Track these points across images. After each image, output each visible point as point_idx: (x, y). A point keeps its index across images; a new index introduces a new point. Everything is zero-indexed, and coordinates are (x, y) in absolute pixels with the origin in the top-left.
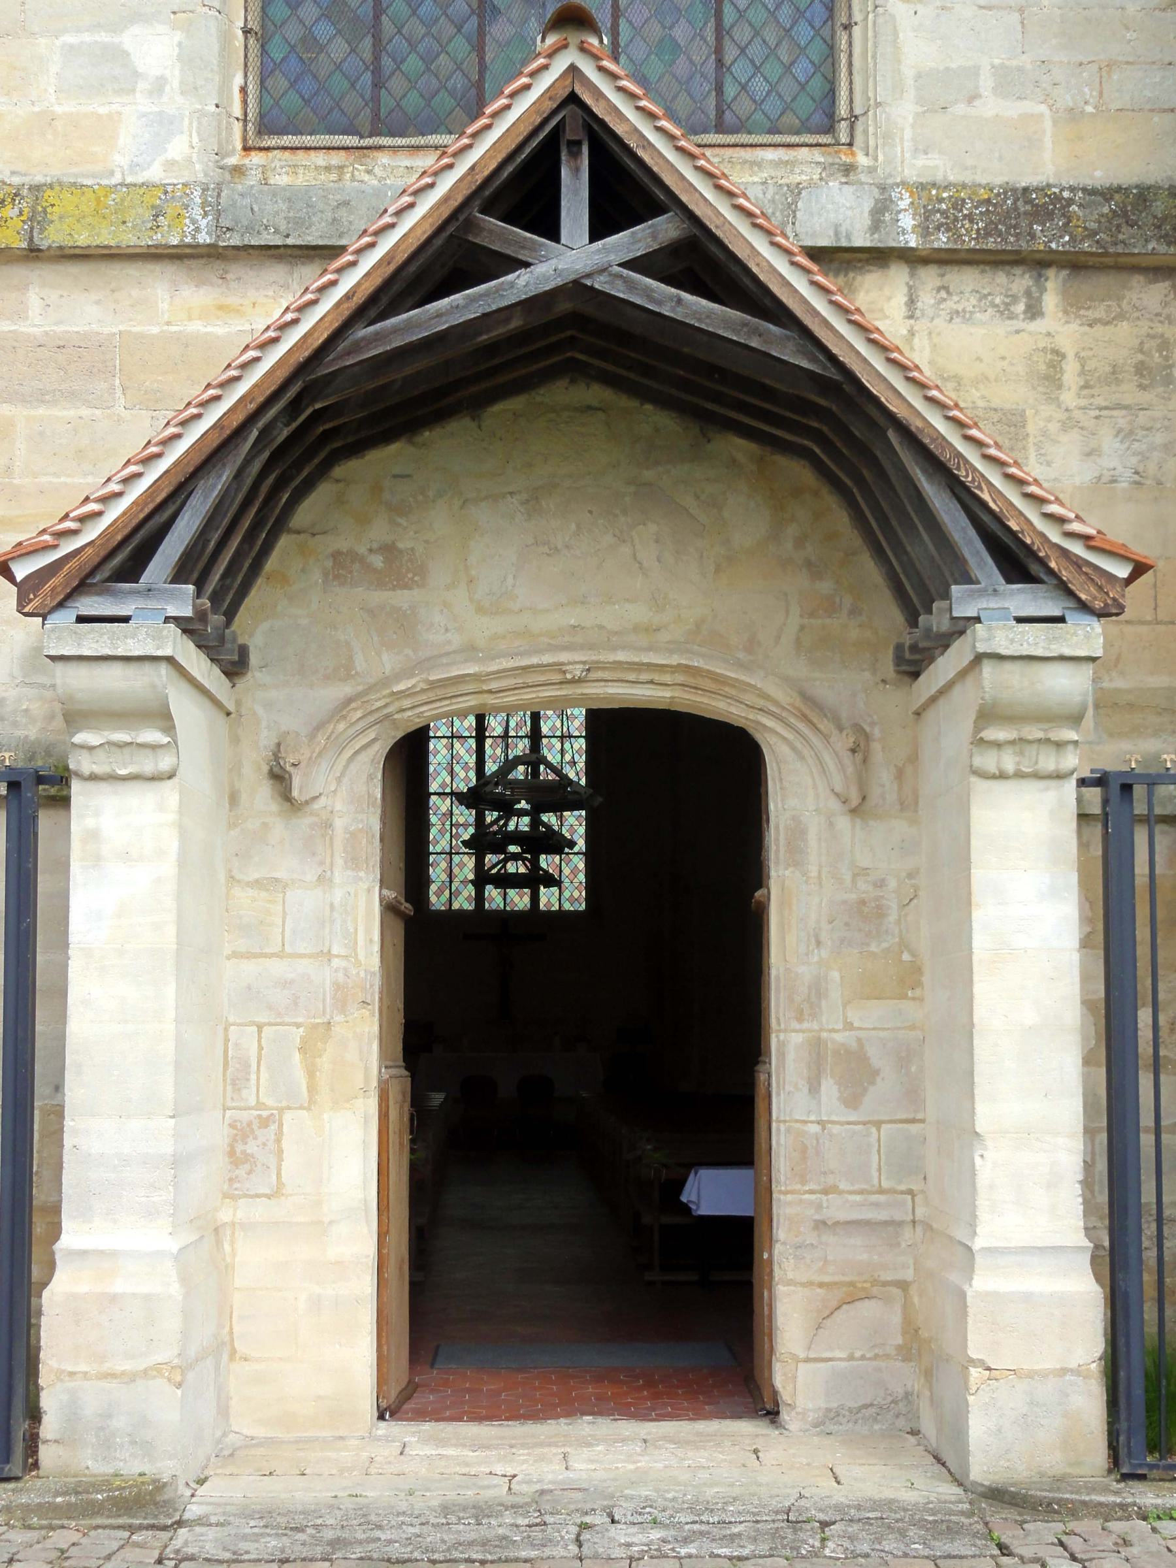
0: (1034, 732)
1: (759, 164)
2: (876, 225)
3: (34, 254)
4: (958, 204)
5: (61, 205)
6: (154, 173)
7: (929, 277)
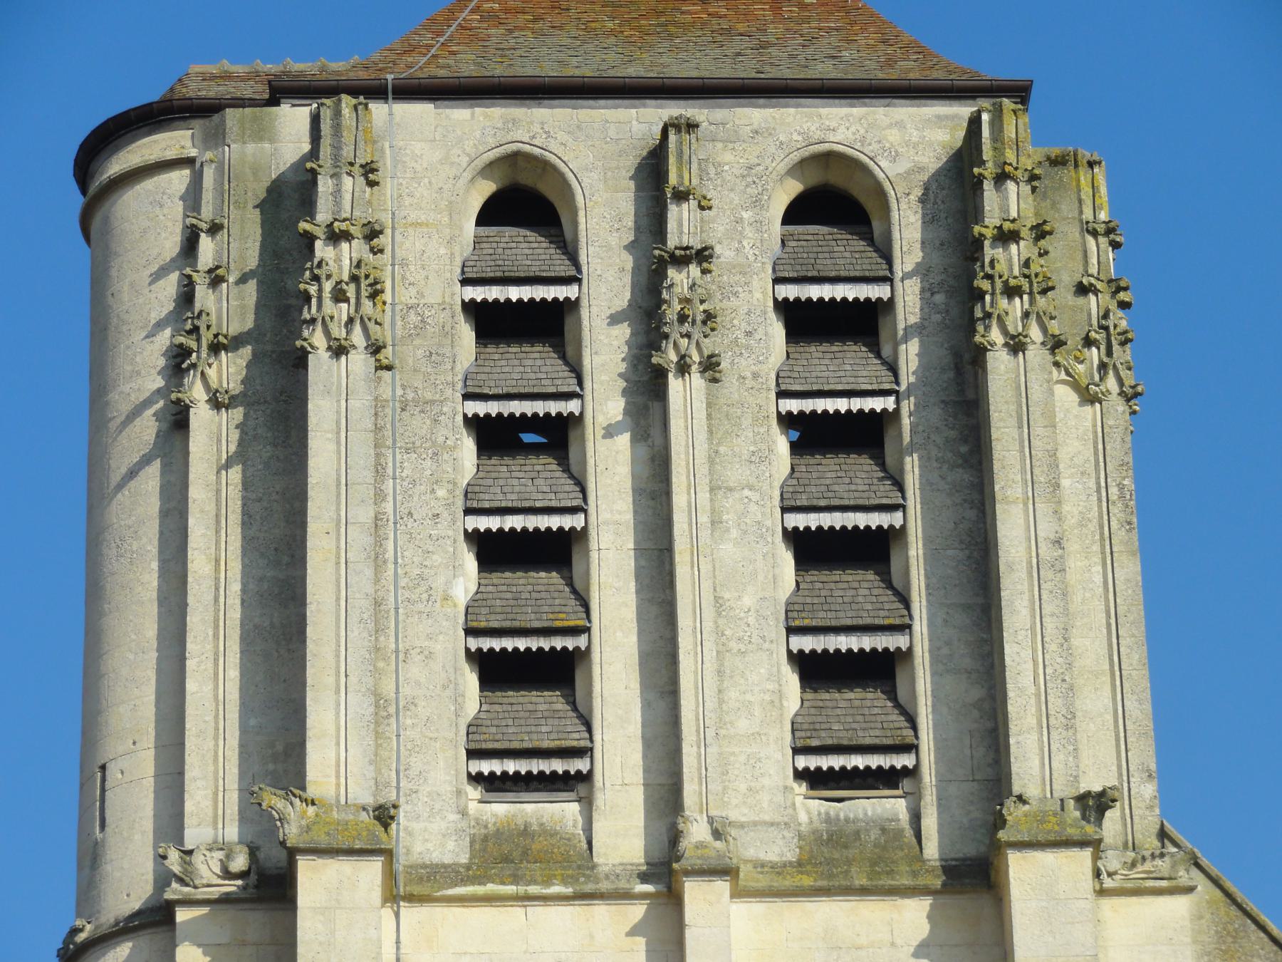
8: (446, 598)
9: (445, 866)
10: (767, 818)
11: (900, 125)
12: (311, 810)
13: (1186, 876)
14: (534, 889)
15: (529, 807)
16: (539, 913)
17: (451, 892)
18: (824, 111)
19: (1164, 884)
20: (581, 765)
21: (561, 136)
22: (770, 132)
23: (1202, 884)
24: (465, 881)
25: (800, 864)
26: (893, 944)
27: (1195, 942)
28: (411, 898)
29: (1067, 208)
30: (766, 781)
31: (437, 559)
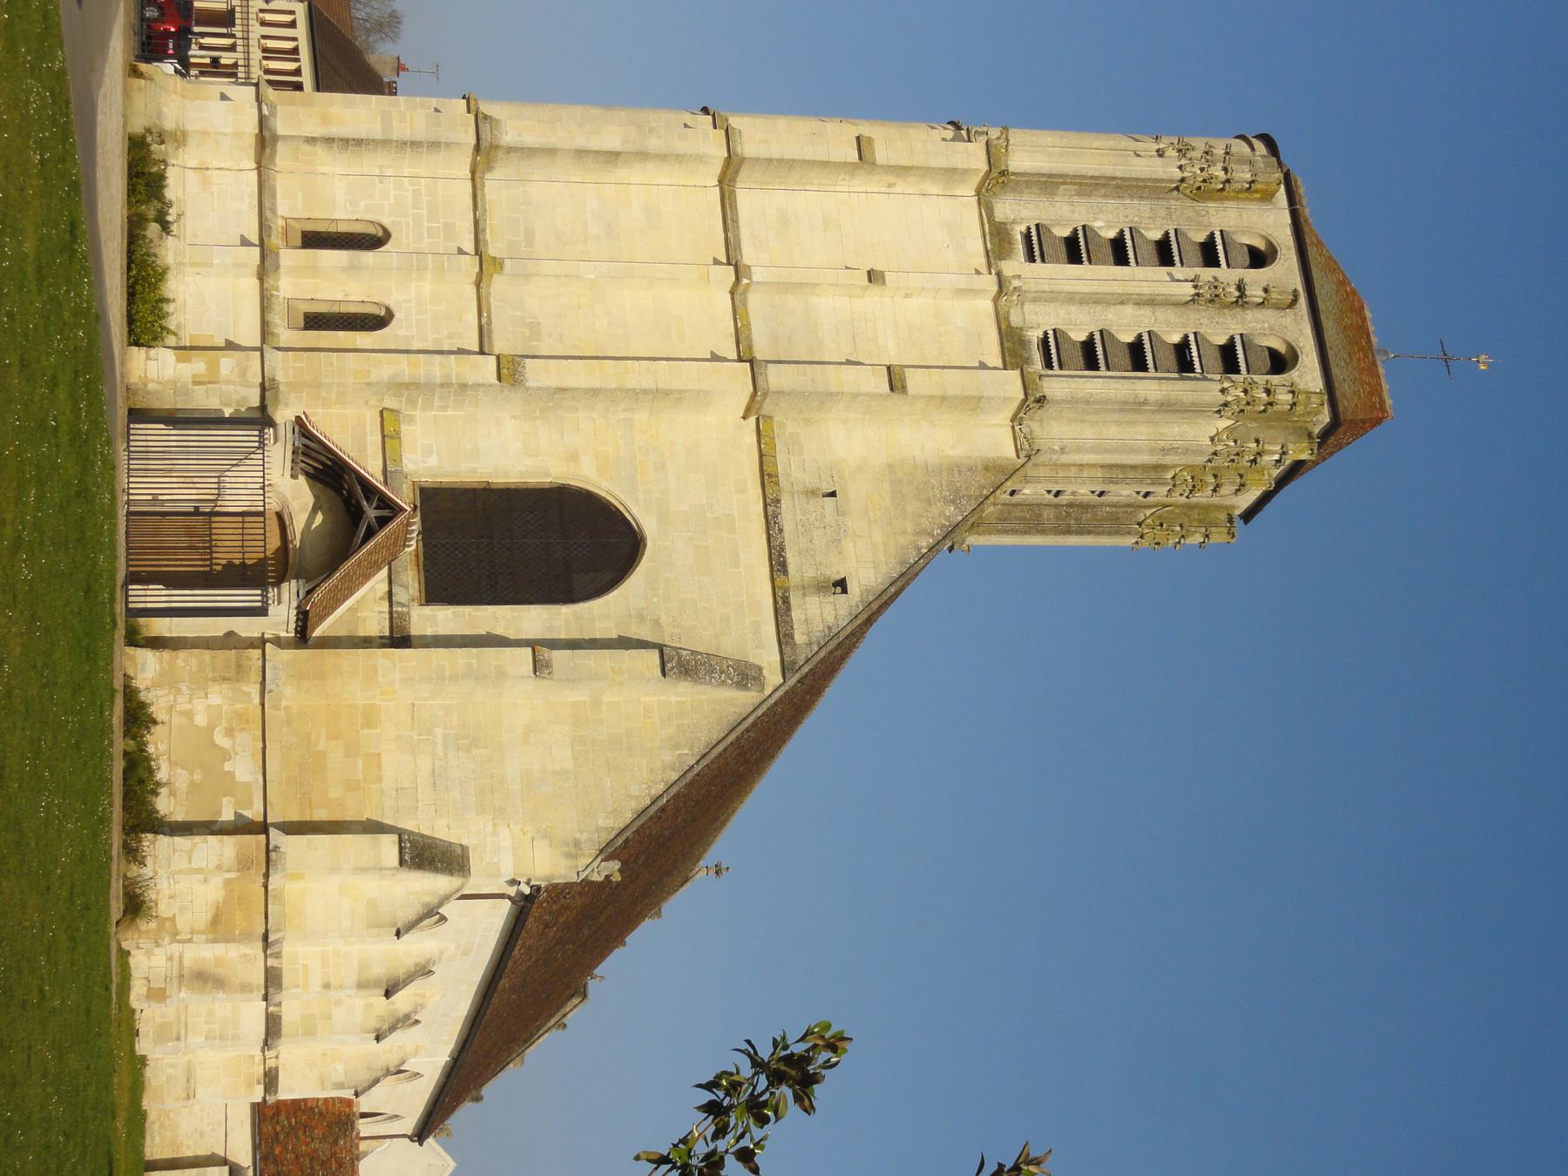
0: (276, 598)
1: (413, 581)
2: (398, 603)
3: (384, 437)
4: (405, 621)
5: (395, 442)
6: (404, 461)
7: (387, 616)
8: (1096, 219)
9: (993, 213)
10: (1026, 317)
11: (1314, 380)
12: (1004, 150)
13: (1022, 454)
14: (988, 238)
16: (980, 241)
17: (983, 211)
18: (1315, 354)
19: (1019, 447)
20: (1038, 258)
21: (1286, 264)
22: (1302, 335)
23: (1023, 460)
24: (989, 222)
25: (1009, 326)
26: (983, 354)
27: (998, 458)
28: (979, 199)
29: (1291, 438)
30: (1041, 318)
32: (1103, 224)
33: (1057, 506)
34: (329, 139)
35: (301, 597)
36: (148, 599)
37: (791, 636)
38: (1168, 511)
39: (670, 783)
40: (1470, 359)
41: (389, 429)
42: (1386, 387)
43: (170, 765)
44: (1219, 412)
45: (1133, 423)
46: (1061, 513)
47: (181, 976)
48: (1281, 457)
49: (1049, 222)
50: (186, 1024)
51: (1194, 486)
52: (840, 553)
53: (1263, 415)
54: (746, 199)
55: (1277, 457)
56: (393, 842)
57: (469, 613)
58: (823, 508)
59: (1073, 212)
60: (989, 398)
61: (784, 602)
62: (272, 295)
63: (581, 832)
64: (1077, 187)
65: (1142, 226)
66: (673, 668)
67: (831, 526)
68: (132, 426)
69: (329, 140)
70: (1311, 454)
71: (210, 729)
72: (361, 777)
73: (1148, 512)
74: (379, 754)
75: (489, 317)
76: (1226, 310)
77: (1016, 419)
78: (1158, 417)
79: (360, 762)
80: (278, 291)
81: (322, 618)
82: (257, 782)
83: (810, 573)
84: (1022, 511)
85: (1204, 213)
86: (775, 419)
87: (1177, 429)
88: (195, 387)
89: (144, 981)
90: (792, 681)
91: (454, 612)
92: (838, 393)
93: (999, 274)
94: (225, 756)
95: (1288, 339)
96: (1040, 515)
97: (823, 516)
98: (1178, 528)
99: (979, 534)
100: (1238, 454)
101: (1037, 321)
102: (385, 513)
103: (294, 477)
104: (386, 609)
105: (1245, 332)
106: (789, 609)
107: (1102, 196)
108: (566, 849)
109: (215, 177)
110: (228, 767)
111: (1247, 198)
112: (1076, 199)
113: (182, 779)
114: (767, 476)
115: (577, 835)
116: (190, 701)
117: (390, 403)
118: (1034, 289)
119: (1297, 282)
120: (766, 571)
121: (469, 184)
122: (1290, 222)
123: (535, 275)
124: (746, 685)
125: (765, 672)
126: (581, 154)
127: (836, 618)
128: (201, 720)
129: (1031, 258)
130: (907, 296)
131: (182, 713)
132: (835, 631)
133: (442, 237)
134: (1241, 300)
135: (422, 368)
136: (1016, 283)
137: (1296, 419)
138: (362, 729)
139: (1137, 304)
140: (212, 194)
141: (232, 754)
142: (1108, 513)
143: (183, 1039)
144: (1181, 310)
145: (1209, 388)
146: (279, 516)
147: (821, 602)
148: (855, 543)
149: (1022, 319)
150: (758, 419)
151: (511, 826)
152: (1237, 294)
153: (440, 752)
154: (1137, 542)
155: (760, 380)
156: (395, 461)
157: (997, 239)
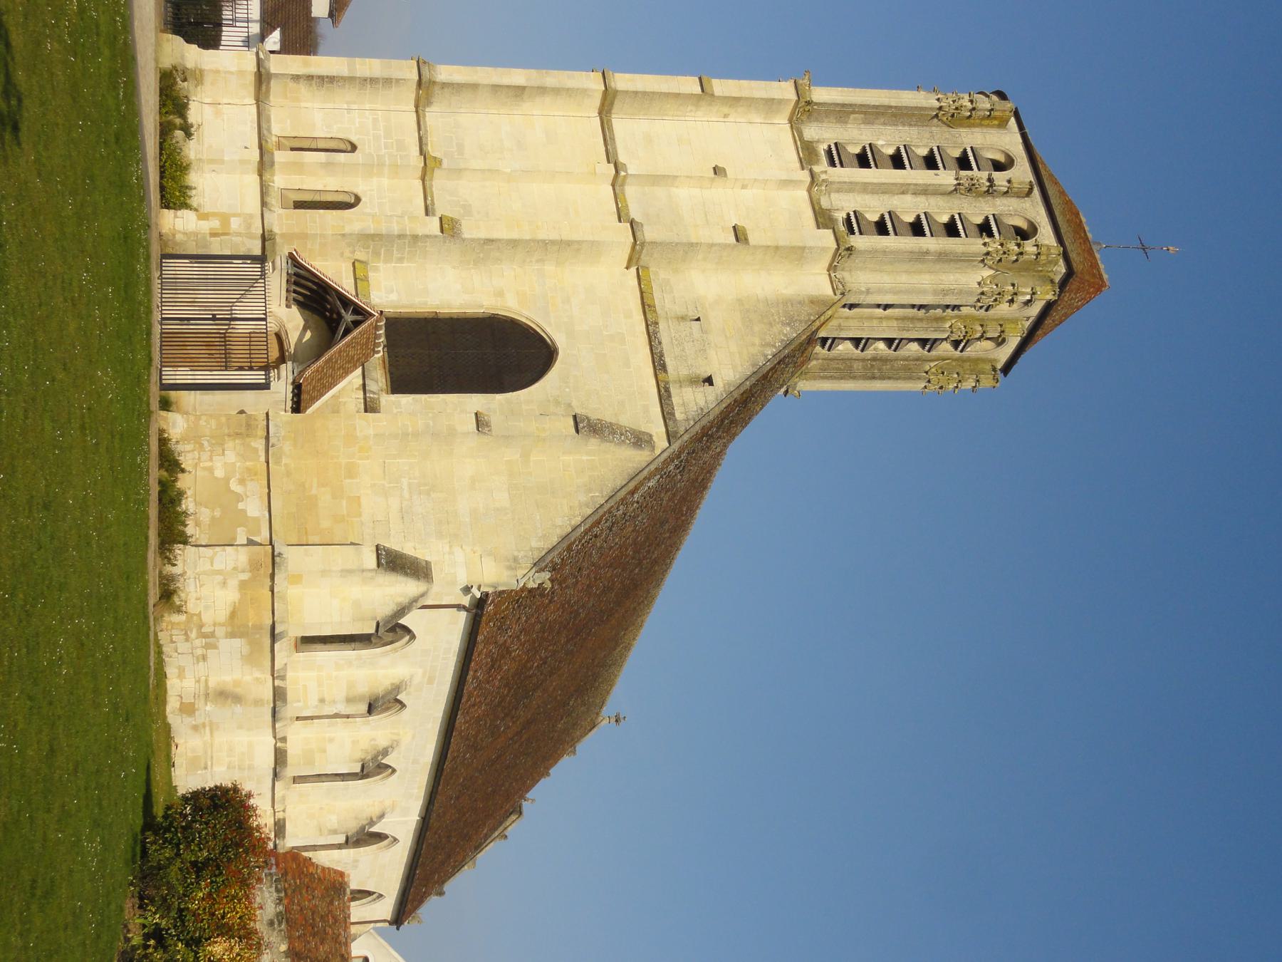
0: (276, 376)
1: (381, 377)
3: (355, 279)
4: (376, 404)
6: (372, 297)
7: (362, 401)
10: (833, 203)
13: (838, 292)
14: (800, 149)
15: (824, 158)
20: (838, 164)
21: (1022, 169)
22: (1039, 215)
23: (839, 297)
24: (800, 140)
25: (821, 208)
28: (792, 126)
29: (1037, 283)
31: (889, 137)
32: (884, 143)
33: (863, 360)
34: (309, 76)
35: (295, 375)
36: (178, 377)
37: (673, 414)
38: (948, 364)
39: (586, 517)
40: (1162, 249)
41: (360, 274)
42: (1102, 266)
43: (196, 504)
44: (983, 261)
45: (920, 272)
46: (867, 366)
47: (207, 695)
48: (1032, 297)
49: (844, 141)
50: (212, 757)
51: (966, 332)
52: (706, 358)
53: (1016, 265)
54: (620, 125)
55: (1028, 297)
56: (372, 551)
57: (425, 399)
58: (691, 328)
59: (861, 134)
60: (810, 248)
61: (666, 391)
62: (269, 185)
63: (519, 551)
64: (862, 116)
65: (913, 144)
66: (584, 427)
67: (698, 340)
68: (164, 261)
69: (310, 78)
70: (1054, 295)
71: (227, 480)
72: (345, 512)
73: (932, 364)
74: (359, 497)
75: (432, 200)
76: (980, 199)
77: (832, 268)
78: (938, 266)
79: (344, 503)
80: (274, 183)
81: (314, 399)
82: (265, 517)
83: (684, 372)
84: (838, 364)
85: (957, 135)
86: (651, 269)
87: (952, 277)
88: (212, 239)
89: (178, 698)
90: (676, 446)
91: (413, 398)
92: (697, 243)
93: (811, 171)
94: (239, 498)
95: (1028, 217)
96: (851, 367)
97: (691, 334)
98: (956, 376)
99: (807, 380)
100: (999, 294)
101: (843, 205)
102: (359, 318)
103: (288, 306)
104: (361, 395)
105: (996, 213)
106: (669, 396)
107: (882, 124)
108: (508, 563)
109: (225, 109)
110: (241, 506)
111: (988, 124)
112: (862, 126)
113: (205, 515)
114: (647, 306)
115: (516, 553)
116: (211, 460)
117: (360, 255)
118: (837, 181)
119: (1030, 177)
120: (651, 370)
121: (414, 115)
122: (1021, 141)
123: (465, 169)
124: (641, 445)
125: (655, 439)
126: (496, 88)
127: (706, 402)
128: (219, 473)
129: (833, 164)
130: (744, 187)
131: (204, 469)
132: (706, 411)
133: (395, 148)
134: (991, 190)
135: (384, 224)
136: (823, 177)
137: (1040, 269)
138: (345, 479)
139: (914, 194)
140: (223, 120)
141: (244, 497)
142: (902, 365)
143: (209, 767)
144: (946, 198)
145: (975, 245)
146: (278, 336)
147: (694, 392)
148: (717, 352)
149: (830, 203)
150: (638, 269)
151: (463, 547)
152: (988, 184)
153: (406, 495)
154: (925, 387)
155: (638, 234)
156: (365, 296)
157: (807, 153)
